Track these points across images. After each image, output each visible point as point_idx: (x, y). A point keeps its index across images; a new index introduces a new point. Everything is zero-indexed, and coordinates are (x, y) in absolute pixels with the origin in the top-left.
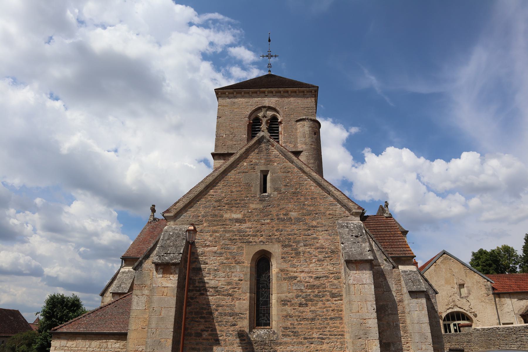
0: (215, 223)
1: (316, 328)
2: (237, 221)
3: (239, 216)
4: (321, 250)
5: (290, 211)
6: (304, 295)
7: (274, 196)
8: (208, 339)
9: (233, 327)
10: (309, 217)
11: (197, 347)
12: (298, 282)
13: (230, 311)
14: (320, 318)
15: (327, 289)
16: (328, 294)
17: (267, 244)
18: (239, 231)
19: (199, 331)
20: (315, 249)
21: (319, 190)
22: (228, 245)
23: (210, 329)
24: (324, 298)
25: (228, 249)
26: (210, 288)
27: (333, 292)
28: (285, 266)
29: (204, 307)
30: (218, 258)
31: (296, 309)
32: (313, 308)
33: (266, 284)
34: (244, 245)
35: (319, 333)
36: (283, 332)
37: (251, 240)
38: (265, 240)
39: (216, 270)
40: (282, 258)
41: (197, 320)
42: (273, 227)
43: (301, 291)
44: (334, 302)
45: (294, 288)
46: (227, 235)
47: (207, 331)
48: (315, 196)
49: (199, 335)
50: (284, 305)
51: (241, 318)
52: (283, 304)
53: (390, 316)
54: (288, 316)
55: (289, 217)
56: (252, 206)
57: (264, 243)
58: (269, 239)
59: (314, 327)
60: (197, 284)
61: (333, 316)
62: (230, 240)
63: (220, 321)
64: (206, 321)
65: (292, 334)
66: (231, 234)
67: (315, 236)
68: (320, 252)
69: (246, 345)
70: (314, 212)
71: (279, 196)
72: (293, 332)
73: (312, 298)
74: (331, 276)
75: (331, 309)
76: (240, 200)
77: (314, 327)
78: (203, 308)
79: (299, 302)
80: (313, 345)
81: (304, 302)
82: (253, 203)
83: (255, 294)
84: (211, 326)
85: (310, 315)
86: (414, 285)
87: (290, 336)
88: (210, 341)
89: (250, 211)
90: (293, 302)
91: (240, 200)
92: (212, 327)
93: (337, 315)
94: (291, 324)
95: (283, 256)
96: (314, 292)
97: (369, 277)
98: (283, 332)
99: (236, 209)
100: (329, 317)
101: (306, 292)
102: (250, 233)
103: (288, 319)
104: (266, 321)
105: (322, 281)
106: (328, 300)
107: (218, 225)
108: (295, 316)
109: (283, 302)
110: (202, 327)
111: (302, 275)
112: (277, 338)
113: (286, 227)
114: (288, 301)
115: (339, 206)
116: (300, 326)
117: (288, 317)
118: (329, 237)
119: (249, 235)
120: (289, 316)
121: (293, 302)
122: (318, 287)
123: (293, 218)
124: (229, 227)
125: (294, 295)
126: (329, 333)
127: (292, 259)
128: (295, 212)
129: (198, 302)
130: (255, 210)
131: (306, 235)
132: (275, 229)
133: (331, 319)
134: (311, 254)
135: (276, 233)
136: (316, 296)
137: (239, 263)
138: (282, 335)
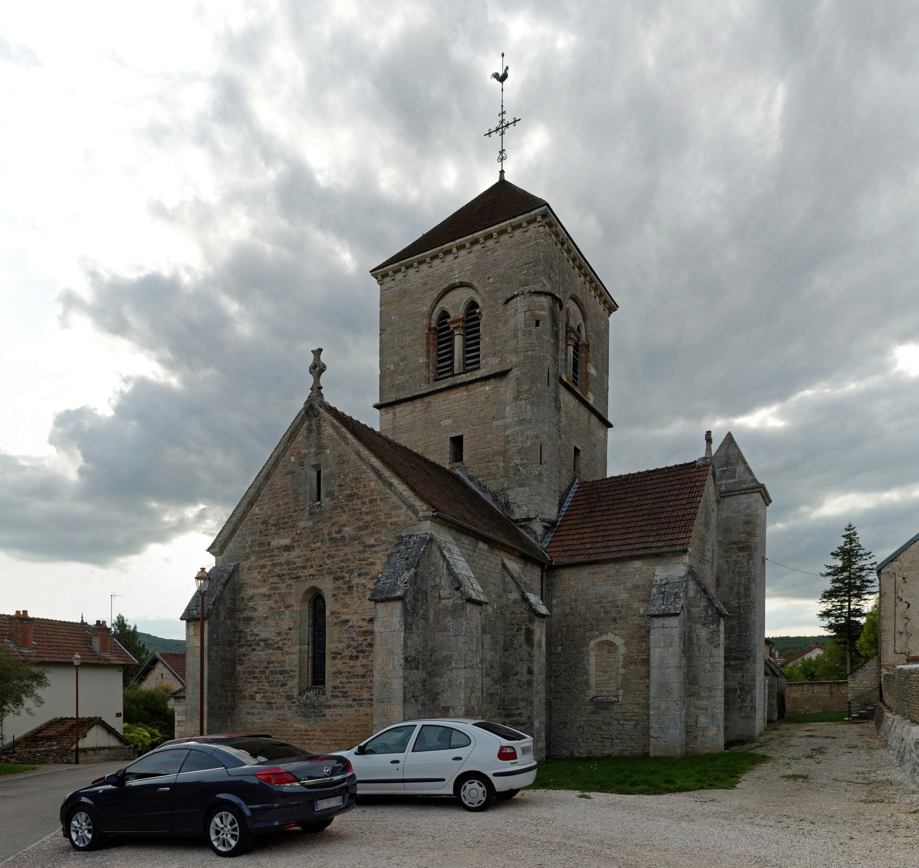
1: (366, 687)
2: (287, 548)
5: (344, 526)
6: (355, 644)
8: (261, 703)
9: (283, 688)
10: (366, 531)
11: (252, 711)
12: (349, 627)
13: (280, 669)
18: (288, 563)
19: (252, 694)
20: (370, 579)
22: (276, 583)
23: (262, 691)
25: (277, 588)
30: (267, 602)
31: (346, 663)
32: (364, 662)
34: (292, 582)
36: (333, 692)
37: (300, 574)
39: (266, 618)
40: (333, 596)
41: (250, 680)
42: (324, 553)
43: (353, 639)
45: (346, 636)
46: (276, 570)
47: (260, 693)
48: (375, 497)
49: (252, 698)
51: (291, 677)
52: (333, 657)
53: (453, 671)
55: (342, 535)
56: (302, 524)
57: (314, 576)
58: (319, 571)
59: (365, 685)
60: (249, 638)
62: (279, 576)
63: (272, 681)
64: (258, 682)
65: (341, 694)
66: (279, 568)
67: (371, 560)
71: (331, 503)
73: (364, 648)
77: (365, 685)
80: (362, 708)
81: (355, 654)
82: (302, 520)
83: (308, 645)
84: (263, 687)
85: (360, 671)
86: (663, 605)
87: (338, 697)
90: (344, 654)
94: (340, 682)
95: (335, 592)
96: (366, 640)
97: (400, 621)
101: (358, 640)
107: (265, 556)
108: (345, 673)
109: (333, 655)
110: (255, 689)
111: (355, 617)
112: (326, 700)
113: (339, 551)
114: (339, 654)
116: (350, 685)
119: (298, 567)
121: (344, 654)
123: (347, 537)
124: (277, 558)
127: (344, 596)
128: (350, 526)
129: (250, 659)
131: (361, 560)
132: (326, 555)
134: (365, 587)
135: (328, 562)
137: (287, 607)
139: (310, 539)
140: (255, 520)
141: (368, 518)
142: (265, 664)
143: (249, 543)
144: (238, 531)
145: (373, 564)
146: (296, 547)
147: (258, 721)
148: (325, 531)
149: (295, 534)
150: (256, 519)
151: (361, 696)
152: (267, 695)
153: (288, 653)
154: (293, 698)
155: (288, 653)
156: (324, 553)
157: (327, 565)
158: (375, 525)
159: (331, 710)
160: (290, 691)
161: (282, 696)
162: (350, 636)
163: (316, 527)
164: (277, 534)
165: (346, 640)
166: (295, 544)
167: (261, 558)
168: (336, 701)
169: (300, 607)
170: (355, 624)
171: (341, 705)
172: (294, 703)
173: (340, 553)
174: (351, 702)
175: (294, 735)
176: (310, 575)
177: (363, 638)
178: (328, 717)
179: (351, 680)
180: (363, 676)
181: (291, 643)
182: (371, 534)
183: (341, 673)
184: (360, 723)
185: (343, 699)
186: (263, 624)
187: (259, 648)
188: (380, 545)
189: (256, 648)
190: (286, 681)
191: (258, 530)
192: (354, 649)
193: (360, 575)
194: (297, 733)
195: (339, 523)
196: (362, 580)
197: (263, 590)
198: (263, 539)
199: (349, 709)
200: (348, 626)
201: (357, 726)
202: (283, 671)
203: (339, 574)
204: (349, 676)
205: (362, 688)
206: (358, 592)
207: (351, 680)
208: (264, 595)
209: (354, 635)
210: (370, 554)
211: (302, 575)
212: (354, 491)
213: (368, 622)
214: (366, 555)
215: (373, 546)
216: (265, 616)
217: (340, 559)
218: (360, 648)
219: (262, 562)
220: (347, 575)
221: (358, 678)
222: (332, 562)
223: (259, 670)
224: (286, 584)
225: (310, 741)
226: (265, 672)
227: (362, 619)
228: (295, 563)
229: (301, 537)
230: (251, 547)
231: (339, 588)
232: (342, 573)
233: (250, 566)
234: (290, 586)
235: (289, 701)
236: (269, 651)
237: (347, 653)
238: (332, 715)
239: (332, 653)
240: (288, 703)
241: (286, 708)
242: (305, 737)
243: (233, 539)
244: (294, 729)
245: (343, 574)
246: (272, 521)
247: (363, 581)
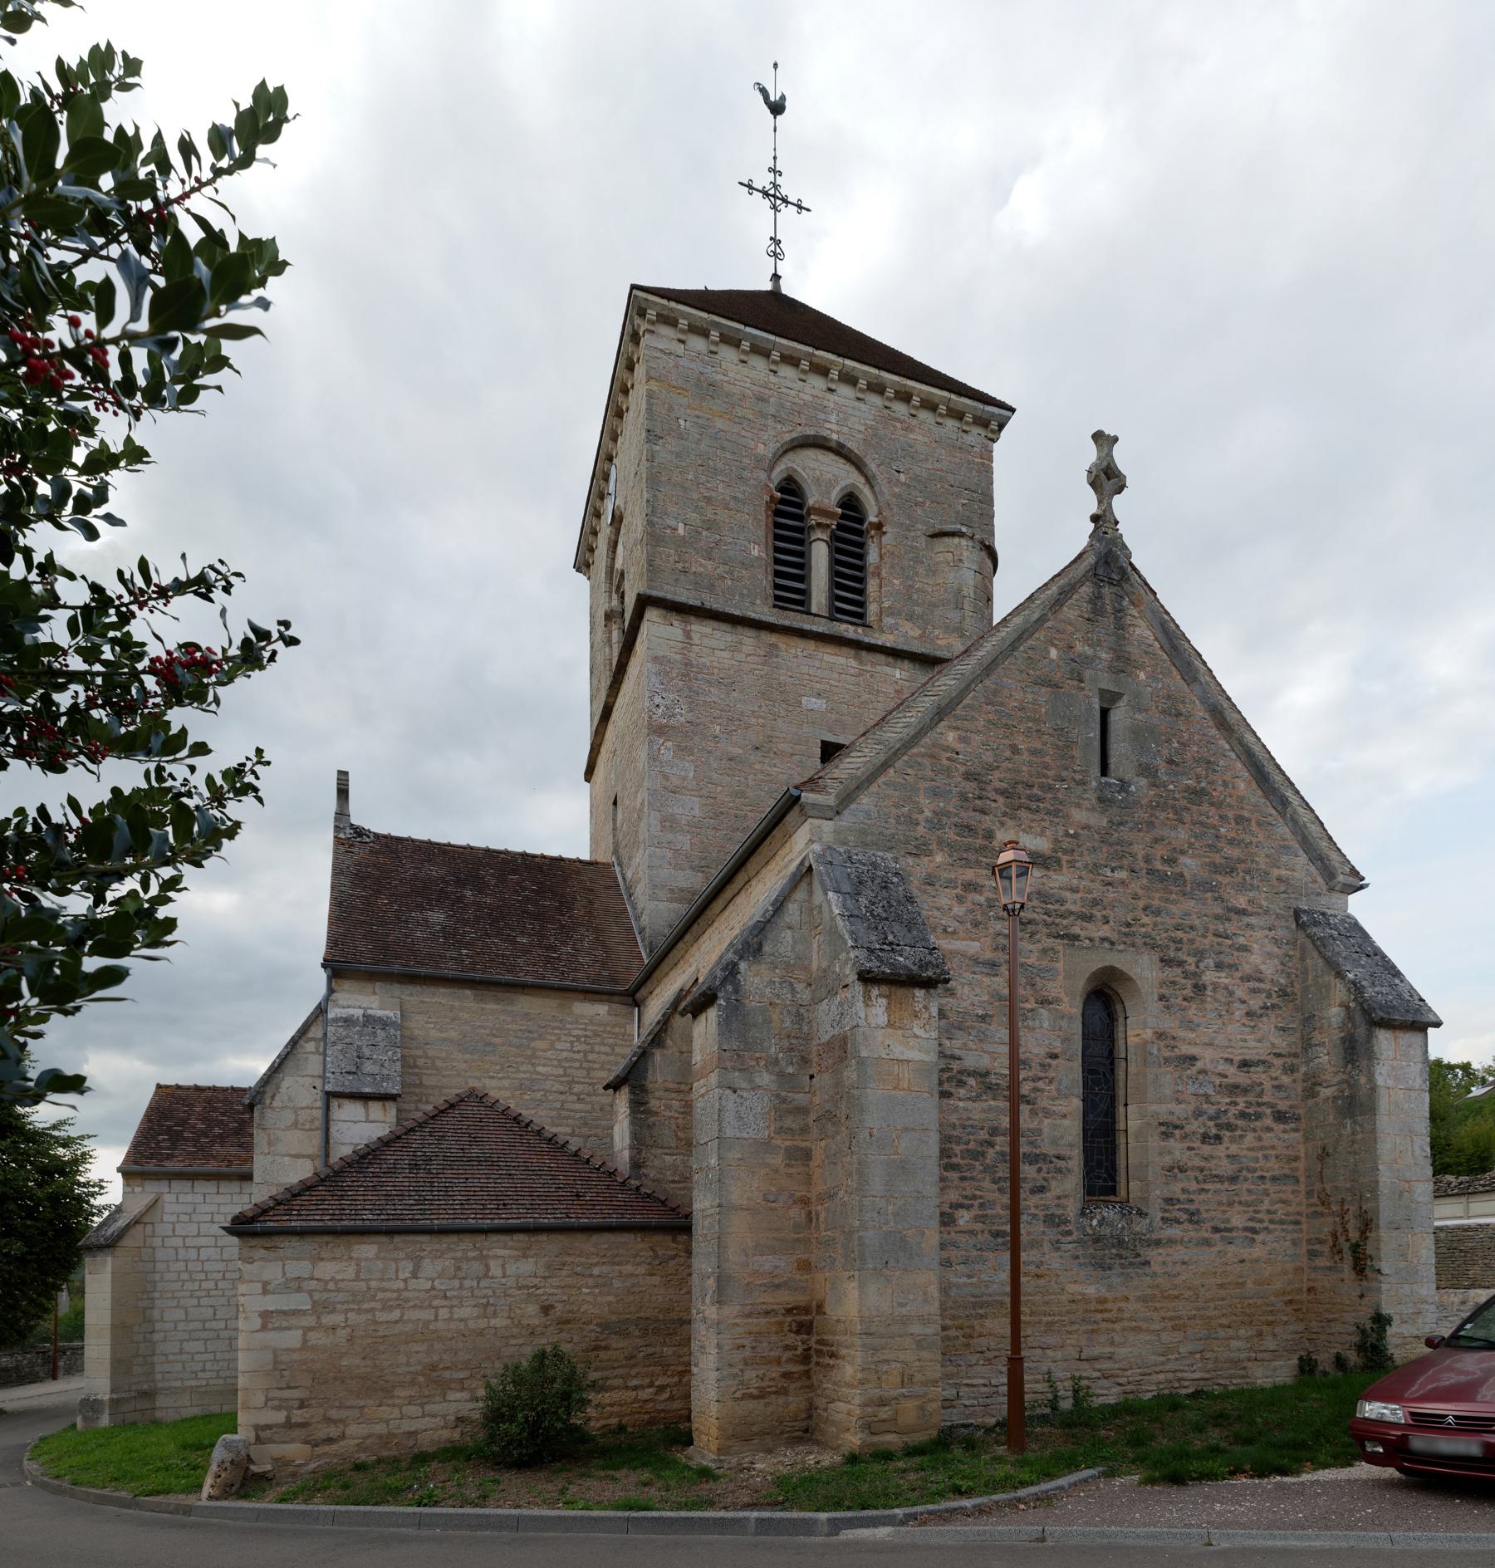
0: (972, 858)
1: (1240, 1203)
3: (1041, 844)
4: (1257, 985)
5: (1182, 852)
6: (1212, 1110)
7: (1138, 790)
8: (972, 1233)
10: (1228, 879)
14: (1250, 1175)
15: (1265, 1099)
16: (1268, 1111)
17: (1121, 951)
20: (1242, 979)
21: (1255, 795)
23: (976, 1203)
24: (1258, 1124)
26: (969, 1075)
27: (1279, 1107)
28: (1169, 1024)
29: (955, 1133)
30: (987, 980)
31: (1193, 1149)
32: (1234, 1149)
34: (1058, 945)
35: (1246, 1216)
36: (1166, 1211)
37: (1076, 930)
38: (1114, 936)
39: (983, 1018)
40: (1161, 999)
42: (1136, 897)
44: (1281, 1135)
45: (1191, 1089)
47: (969, 1207)
50: (1166, 1135)
51: (1059, 1171)
52: (1163, 1133)
54: (1176, 1169)
55: (1177, 870)
56: (1079, 816)
57: (1112, 943)
59: (1237, 1199)
61: (1277, 1173)
64: (963, 1179)
65: (1185, 1217)
67: (1242, 940)
68: (1254, 991)
69: (1076, 1248)
70: (1243, 866)
72: (1186, 1211)
73: (1232, 1121)
74: (1278, 1062)
75: (1273, 1153)
76: (1042, 787)
77: (1237, 1199)
78: (950, 1137)
79: (1202, 1131)
80: (1231, 1249)
81: (1214, 1131)
82: (1078, 805)
84: (977, 1193)
85: (1226, 1168)
88: (979, 1236)
89: (1072, 832)
90: (1188, 1129)
91: (1042, 787)
92: (981, 1197)
93: (1287, 1172)
95: (1164, 991)
96: (1235, 1104)
98: (1166, 1211)
99: (1031, 816)
100: (1268, 1175)
101: (1219, 1103)
102: (1073, 908)
103: (1175, 1177)
105: (1257, 1075)
106: (1269, 1129)
107: (978, 863)
109: (1163, 1129)
113: (1172, 902)
114: (1176, 1127)
115: (1303, 858)
116: (1203, 1196)
117: (1176, 1170)
118: (1276, 950)
119: (1072, 913)
120: (1179, 1168)
121: (1188, 1129)
122: (1245, 1091)
123: (1188, 877)
125: (1191, 1108)
126: (1266, 1217)
127: (1185, 1003)
128: (1193, 856)
130: (1086, 832)
131: (1221, 936)
132: (1141, 904)
133: (1274, 1179)
134: (1231, 993)
135: (1145, 920)
136: (1243, 1115)
137: (1044, 1002)
138: (1162, 1218)
139: (1101, 856)
140: (945, 762)
141: (1236, 853)
142: (983, 1135)
143: (928, 813)
144: (891, 771)
145: (1245, 949)
146: (1064, 863)
147: (965, 1280)
148: (1139, 849)
149: (1061, 833)
150: (948, 759)
151: (1228, 1221)
152: (989, 1212)
153: (1048, 1113)
154: (1066, 1222)
155: (1048, 1113)
156: (1136, 897)
157: (1143, 926)
158: (1248, 872)
159: (1160, 1251)
160: (1058, 1206)
161: (1034, 1216)
163: (1116, 835)
164: (1013, 817)
165: (1192, 1099)
166: (1065, 858)
167: (967, 863)
168: (1174, 1232)
170: (1209, 1066)
171: (1186, 1239)
172: (1069, 1233)
173: (1174, 909)
174: (1207, 1235)
175: (1068, 1312)
176: (1103, 940)
177: (1228, 1100)
178: (1155, 1267)
179: (1207, 1186)
180: (1233, 1179)
181: (1058, 1090)
182: (1242, 887)
183: (1182, 1170)
184: (1229, 1280)
185: (1191, 1227)
186: (974, 1033)
187: (962, 1092)
188: (1259, 914)
189: (952, 1090)
190: (1045, 1179)
191: (955, 790)
192: (1210, 1119)
193: (1219, 966)
194: (1074, 1306)
195: (1170, 843)
196: (1223, 978)
197: (973, 947)
198: (969, 817)
199: (1205, 1248)
200: (1194, 1070)
201: (1221, 1286)
202: (1037, 1155)
203: (1172, 954)
204: (1200, 1178)
205: (1230, 1204)
206: (1216, 1000)
207: (1207, 1186)
208: (976, 961)
209: (1211, 1092)
210: (1239, 928)
211: (1083, 933)
212: (1203, 785)
213: (1239, 1067)
214: (1231, 928)
215: (1243, 912)
216: (980, 1012)
217: (1174, 921)
218: (1223, 1120)
219: (969, 875)
220: (1191, 960)
221: (1222, 1182)
222: (1155, 925)
223: (963, 1147)
224: (1040, 946)
225: (1110, 1325)
226: (983, 1154)
227: (1226, 1060)
228: (1062, 902)
229: (1079, 846)
230: (935, 824)
231: (1173, 983)
232: (1180, 954)
233: (929, 876)
234: (1050, 953)
235: (1055, 1230)
236: (992, 1103)
237: (1194, 1126)
238: (1164, 1263)
239: (1161, 1124)
240: (1052, 1234)
241: (1046, 1247)
242: (1099, 1316)
243: (874, 788)
244: (1070, 1297)
245: (1182, 956)
246: (996, 779)
247: (1226, 981)
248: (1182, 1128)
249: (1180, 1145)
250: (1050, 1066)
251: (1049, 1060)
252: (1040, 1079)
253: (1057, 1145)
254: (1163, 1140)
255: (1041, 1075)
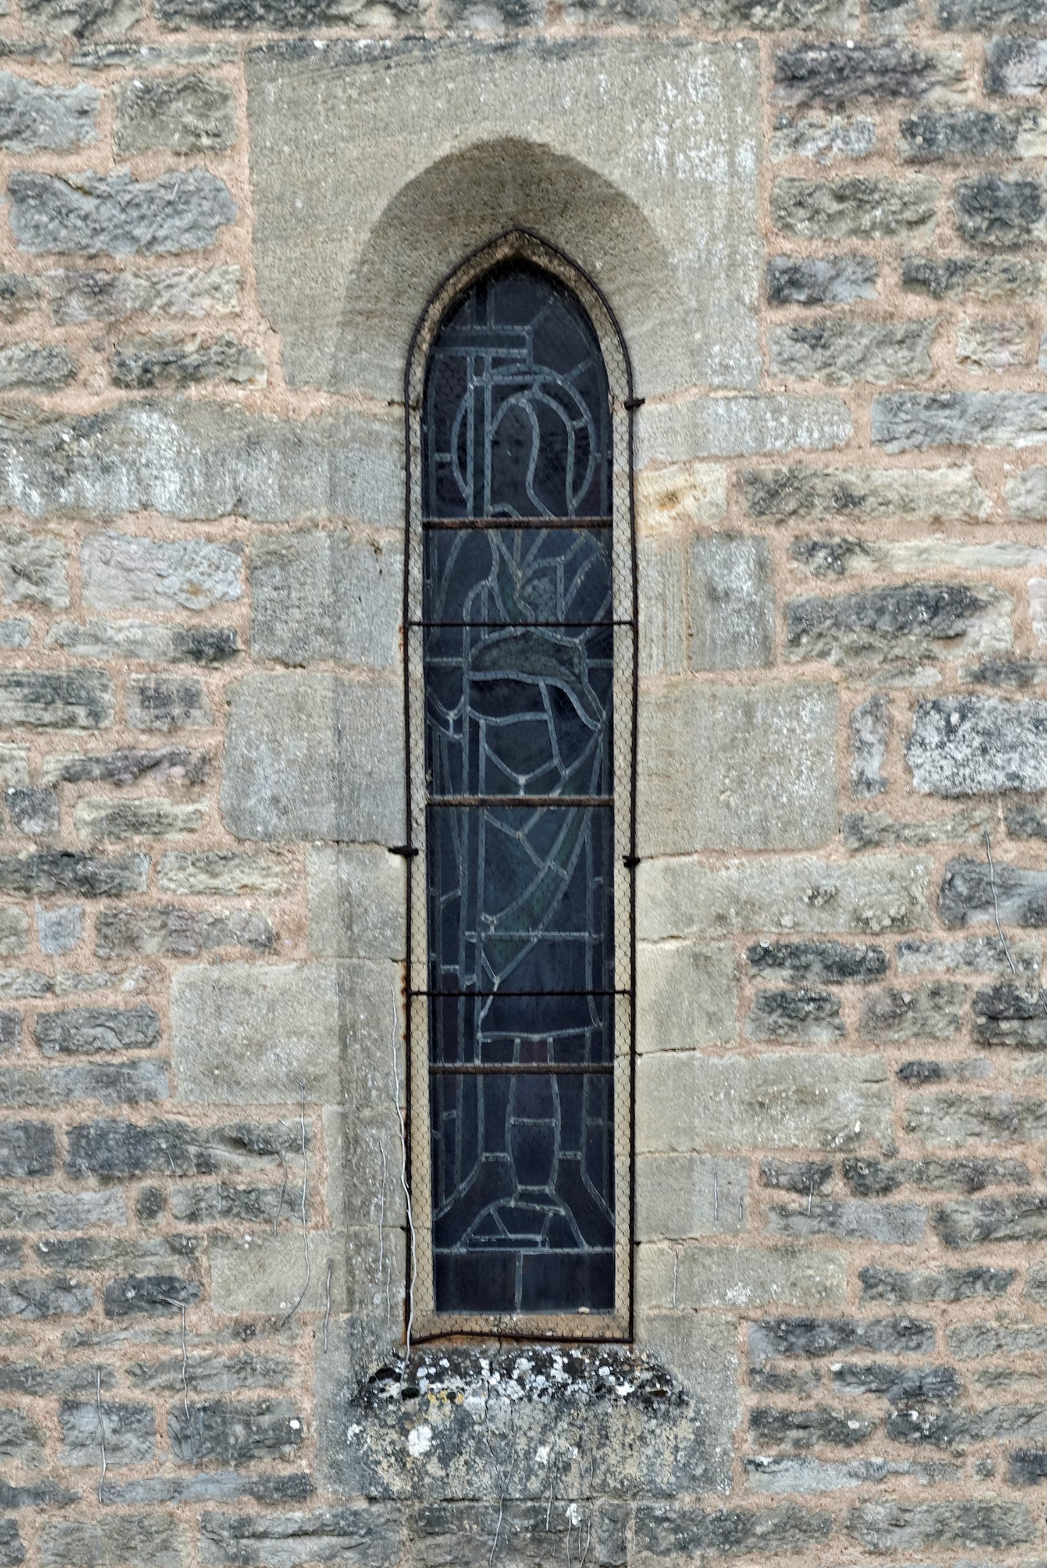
31: (934, 1074)
33: (559, 699)
79: (983, 981)
83: (407, 853)
104: (560, 1235)
109: (776, 980)
117: (836, 1186)
120: (850, 1172)
162: (989, 778)
169: (335, 380)
181: (234, 817)
202: (137, 1136)
239: (762, 957)
248: (879, 968)
249: (864, 1061)
250: (190, 697)
251: (188, 672)
252: (146, 767)
253: (234, 1083)
254: (774, 1032)
255: (155, 746)
